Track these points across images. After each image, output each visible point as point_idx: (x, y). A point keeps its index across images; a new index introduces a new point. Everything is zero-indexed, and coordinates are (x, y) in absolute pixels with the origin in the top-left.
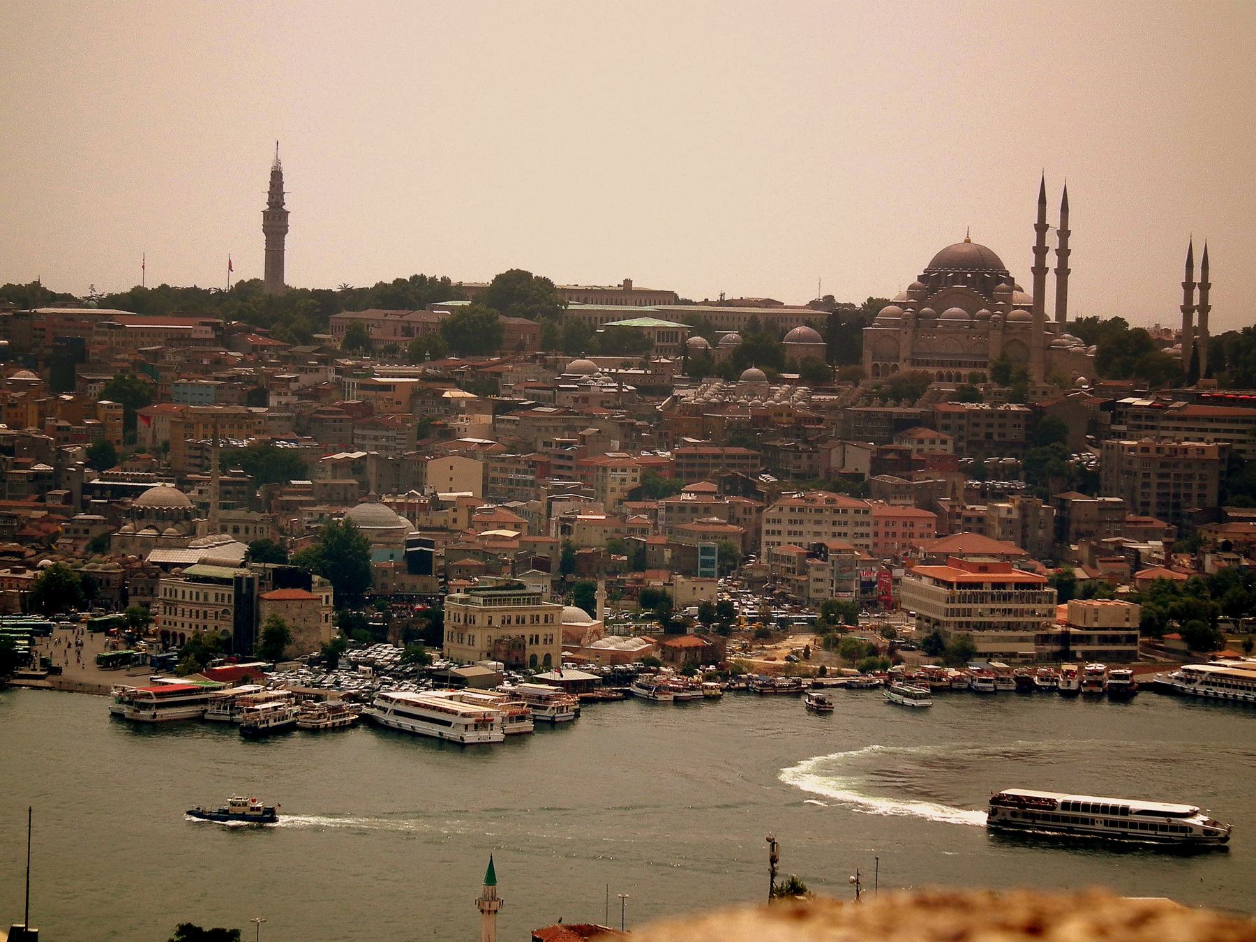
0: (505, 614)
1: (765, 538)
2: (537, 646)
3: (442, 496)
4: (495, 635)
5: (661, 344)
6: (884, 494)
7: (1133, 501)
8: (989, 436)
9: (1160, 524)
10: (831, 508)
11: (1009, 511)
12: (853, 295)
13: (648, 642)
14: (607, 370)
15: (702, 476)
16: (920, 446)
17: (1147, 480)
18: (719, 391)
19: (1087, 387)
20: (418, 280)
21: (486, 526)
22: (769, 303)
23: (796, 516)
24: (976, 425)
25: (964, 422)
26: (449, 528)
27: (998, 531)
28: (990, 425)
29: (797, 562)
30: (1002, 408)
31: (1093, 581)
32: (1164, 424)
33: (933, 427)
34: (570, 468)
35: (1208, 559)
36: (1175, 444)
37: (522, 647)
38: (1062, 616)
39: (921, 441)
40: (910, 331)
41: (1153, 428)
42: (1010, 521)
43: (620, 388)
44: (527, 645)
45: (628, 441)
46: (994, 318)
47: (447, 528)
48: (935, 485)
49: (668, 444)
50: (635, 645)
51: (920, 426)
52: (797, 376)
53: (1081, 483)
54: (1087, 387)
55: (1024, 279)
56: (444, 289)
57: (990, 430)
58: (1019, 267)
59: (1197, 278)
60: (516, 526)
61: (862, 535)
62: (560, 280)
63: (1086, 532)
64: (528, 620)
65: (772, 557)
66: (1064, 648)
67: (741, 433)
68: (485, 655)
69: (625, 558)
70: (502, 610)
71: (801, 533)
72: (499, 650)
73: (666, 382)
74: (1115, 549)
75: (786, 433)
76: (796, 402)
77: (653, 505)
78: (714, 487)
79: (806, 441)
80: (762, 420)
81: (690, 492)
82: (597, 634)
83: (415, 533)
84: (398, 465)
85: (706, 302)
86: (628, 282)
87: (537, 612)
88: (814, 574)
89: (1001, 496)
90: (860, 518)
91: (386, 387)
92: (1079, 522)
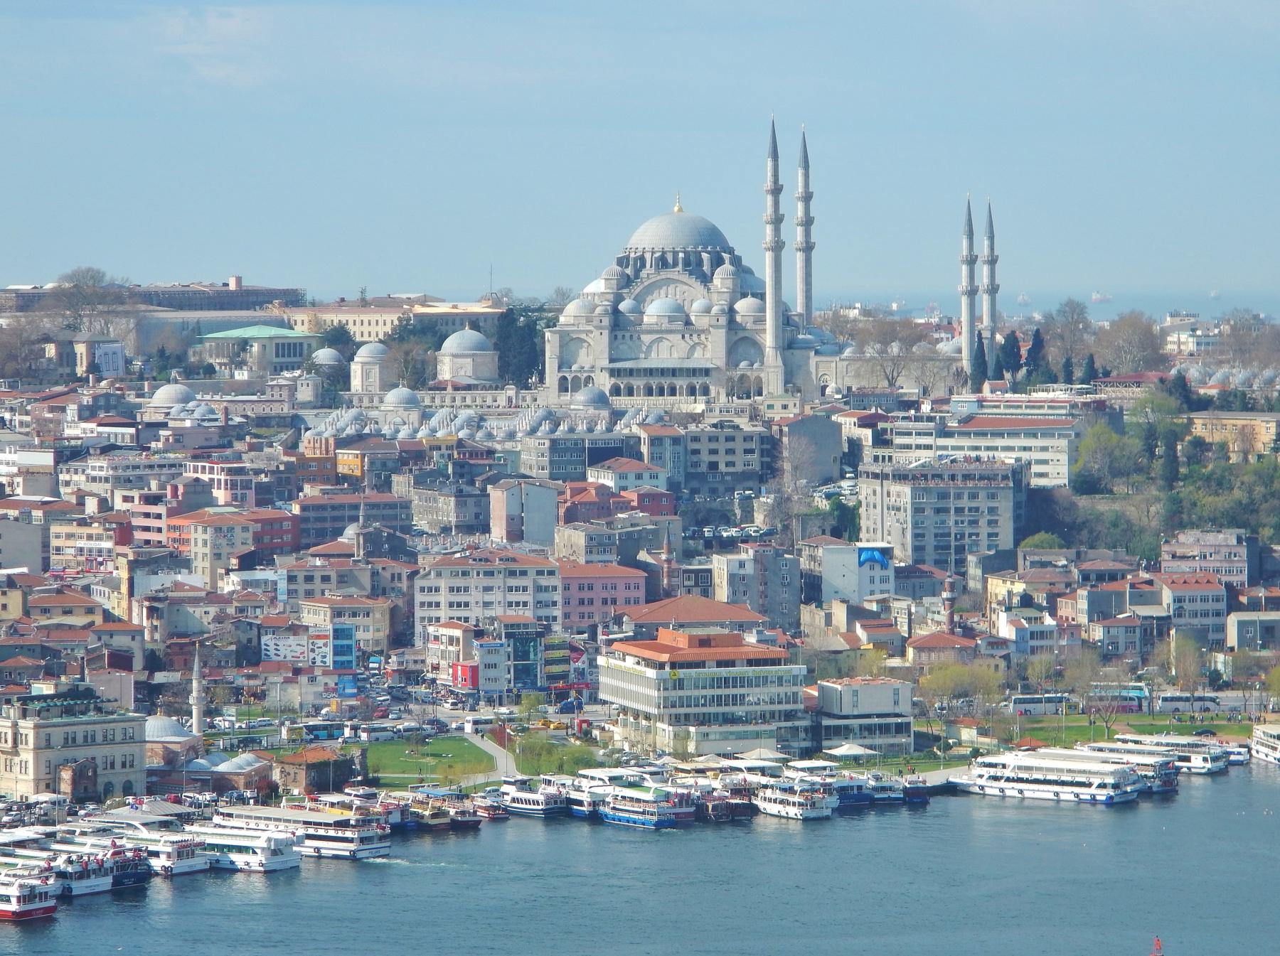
1: (419, 613)
2: (112, 771)
5: (281, 360)
8: (713, 466)
24: (696, 452)
28: (714, 452)
34: (160, 530)
40: (606, 333)
49: (290, 491)
57: (713, 458)
66: (815, 744)
68: (43, 786)
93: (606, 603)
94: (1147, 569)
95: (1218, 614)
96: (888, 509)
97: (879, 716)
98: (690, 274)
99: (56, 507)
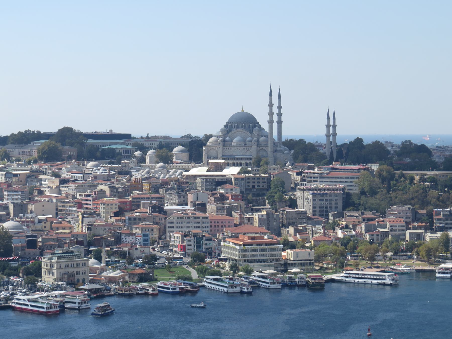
0: (66, 263)
1: (168, 230)
2: (79, 275)
4: (63, 271)
8: (253, 187)
10: (193, 217)
19: (291, 166)
21: (58, 229)
23: (179, 220)
24: (248, 182)
25: (244, 181)
26: (43, 230)
28: (254, 182)
31: (295, 242)
34: (90, 205)
40: (221, 147)
44: (75, 275)
47: (42, 230)
48: (233, 207)
49: (128, 194)
53: (290, 204)
55: (265, 126)
56: (38, 136)
57: (254, 184)
59: (331, 123)
61: (205, 227)
63: (292, 223)
64: (75, 265)
66: (285, 268)
68: (59, 279)
70: (65, 262)
71: (182, 227)
72: (64, 278)
73: (127, 169)
77: (123, 218)
81: (138, 212)
82: (103, 270)
84: (22, 206)
87: (79, 262)
90: (205, 220)
91: (16, 175)
93: (222, 227)
94: (382, 217)
95: (403, 230)
97: (304, 260)
98: (246, 130)
99: (59, 197)
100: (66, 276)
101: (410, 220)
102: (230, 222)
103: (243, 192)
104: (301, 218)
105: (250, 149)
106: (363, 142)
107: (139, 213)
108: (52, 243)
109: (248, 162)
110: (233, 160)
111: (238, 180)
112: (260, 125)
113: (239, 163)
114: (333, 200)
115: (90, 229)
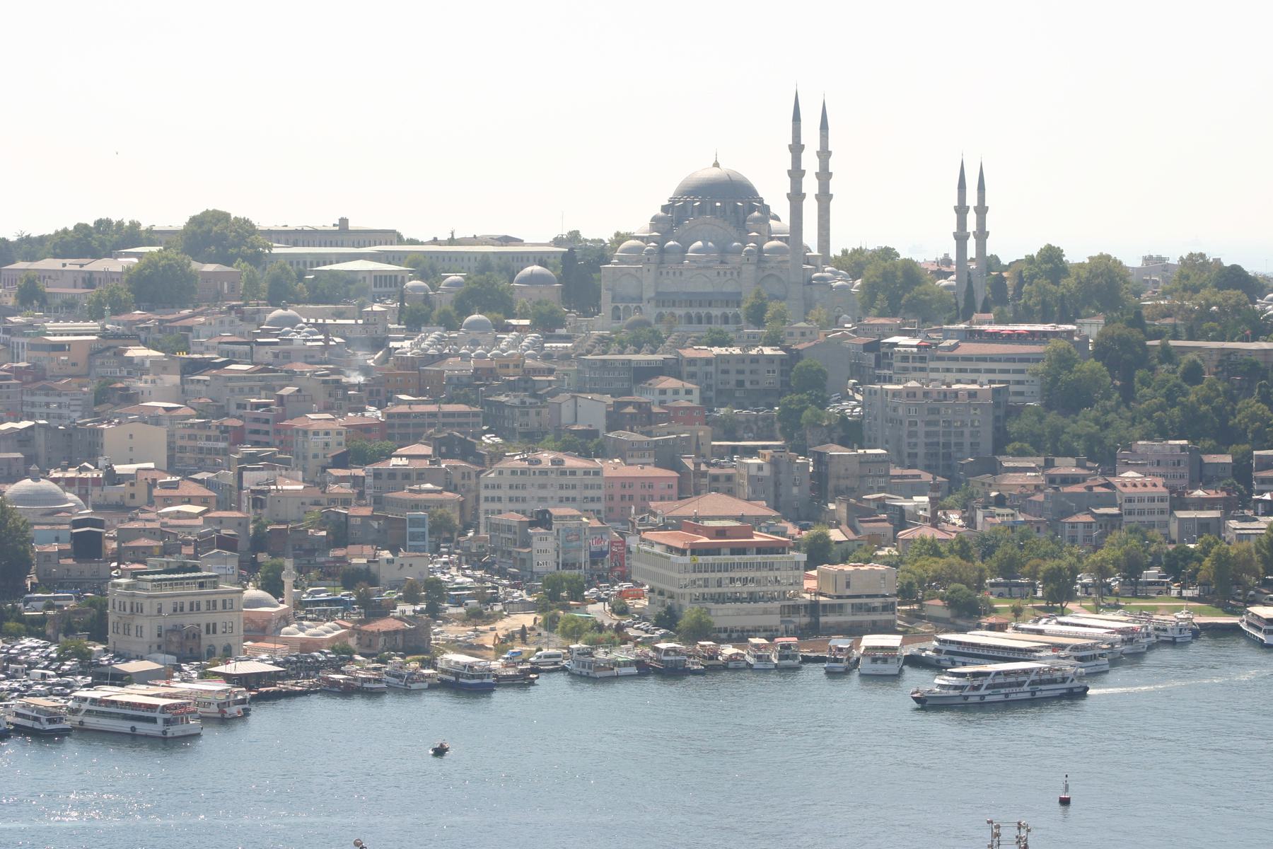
0: (178, 600)
1: (483, 506)
2: (215, 636)
3: (119, 470)
4: (168, 621)
5: (378, 289)
6: (622, 452)
7: (899, 453)
8: (740, 384)
9: (927, 477)
10: (557, 469)
11: (760, 467)
12: (597, 230)
13: (343, 627)
14: (312, 321)
15: (416, 439)
16: (663, 397)
17: (913, 429)
18: (440, 340)
19: (850, 325)
20: (103, 224)
21: (168, 501)
22: (507, 240)
23: (517, 479)
24: (726, 372)
25: (711, 369)
26: (127, 505)
27: (747, 490)
28: (740, 372)
29: (518, 531)
30: (754, 352)
31: (850, 543)
32: (933, 365)
33: (679, 376)
34: (267, 433)
35: (980, 515)
36: (944, 387)
37: (196, 636)
38: (810, 584)
39: (663, 392)
40: (653, 267)
41: (922, 369)
42: (760, 479)
43: (327, 340)
44: (203, 635)
45: (332, 400)
46: (647, 251)
47: (124, 504)
48: (679, 441)
49: (380, 401)
50: (326, 630)
51: (663, 375)
52: (527, 322)
53: (843, 434)
54: (850, 325)
55: (780, 206)
56: (130, 236)
57: (741, 377)
58: (774, 195)
59: (972, 200)
60: (202, 501)
61: (592, 500)
62: (264, 220)
63: (847, 488)
64: (203, 607)
65: (495, 528)
66: (813, 620)
67: (463, 388)
68: (155, 647)
69: (324, 533)
70: (173, 596)
71: (524, 500)
72: (170, 641)
73: (379, 332)
74: (878, 507)
75: (511, 387)
76: (526, 351)
77: (359, 472)
78: (427, 450)
79: (534, 395)
80: (484, 374)
81: (401, 456)
82: (285, 620)
83: (87, 512)
84: (70, 435)
85: (435, 241)
86: (344, 221)
87: (214, 597)
88: (537, 544)
89: (752, 452)
90: (590, 479)
91: (60, 347)
92: (838, 478)
93: (644, 499)
94: (1103, 474)
95: (1162, 512)
96: (887, 421)
97: (868, 596)
98: (725, 220)
99: (179, 412)
100: (175, 639)
101: (1185, 482)
102: (627, 486)
103: (710, 399)
104: (873, 476)
105: (735, 274)
106: (1064, 255)
107: (404, 459)
108: (144, 542)
109: (730, 311)
110: (686, 307)
111: (695, 365)
112: (768, 207)
113: (703, 315)
114: (967, 424)
115: (259, 505)
